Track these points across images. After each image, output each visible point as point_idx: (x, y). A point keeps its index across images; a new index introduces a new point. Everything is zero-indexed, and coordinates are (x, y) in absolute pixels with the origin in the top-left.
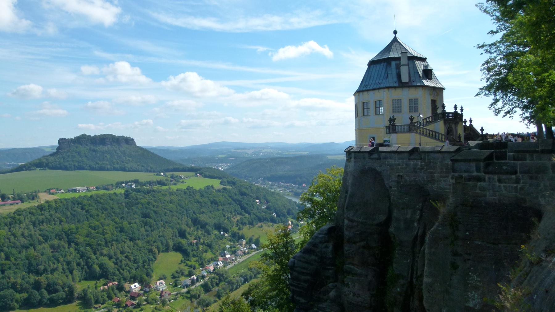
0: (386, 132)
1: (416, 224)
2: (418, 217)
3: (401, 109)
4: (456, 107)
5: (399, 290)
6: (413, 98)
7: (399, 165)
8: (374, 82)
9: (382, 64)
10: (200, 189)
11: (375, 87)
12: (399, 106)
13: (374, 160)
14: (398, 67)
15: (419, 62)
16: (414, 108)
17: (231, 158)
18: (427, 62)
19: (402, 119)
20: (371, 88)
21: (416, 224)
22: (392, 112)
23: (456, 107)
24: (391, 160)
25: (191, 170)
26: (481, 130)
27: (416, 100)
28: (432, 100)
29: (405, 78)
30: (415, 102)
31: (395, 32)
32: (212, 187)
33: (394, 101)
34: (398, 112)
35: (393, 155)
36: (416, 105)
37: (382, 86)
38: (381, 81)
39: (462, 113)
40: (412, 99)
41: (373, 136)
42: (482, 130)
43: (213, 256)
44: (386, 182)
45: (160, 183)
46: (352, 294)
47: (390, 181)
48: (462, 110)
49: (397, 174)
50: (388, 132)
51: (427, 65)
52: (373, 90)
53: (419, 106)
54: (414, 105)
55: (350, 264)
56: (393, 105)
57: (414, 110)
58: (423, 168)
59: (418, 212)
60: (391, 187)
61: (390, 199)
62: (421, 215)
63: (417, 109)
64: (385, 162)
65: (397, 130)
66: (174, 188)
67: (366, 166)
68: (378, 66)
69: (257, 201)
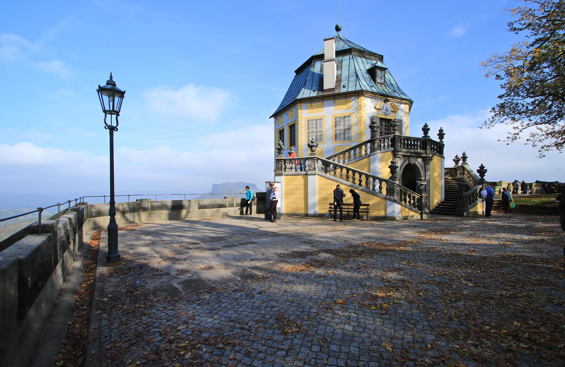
4: (426, 129)
12: (318, 129)
23: (426, 129)
26: (478, 171)
33: (310, 122)
39: (441, 141)
42: (482, 171)
48: (441, 135)
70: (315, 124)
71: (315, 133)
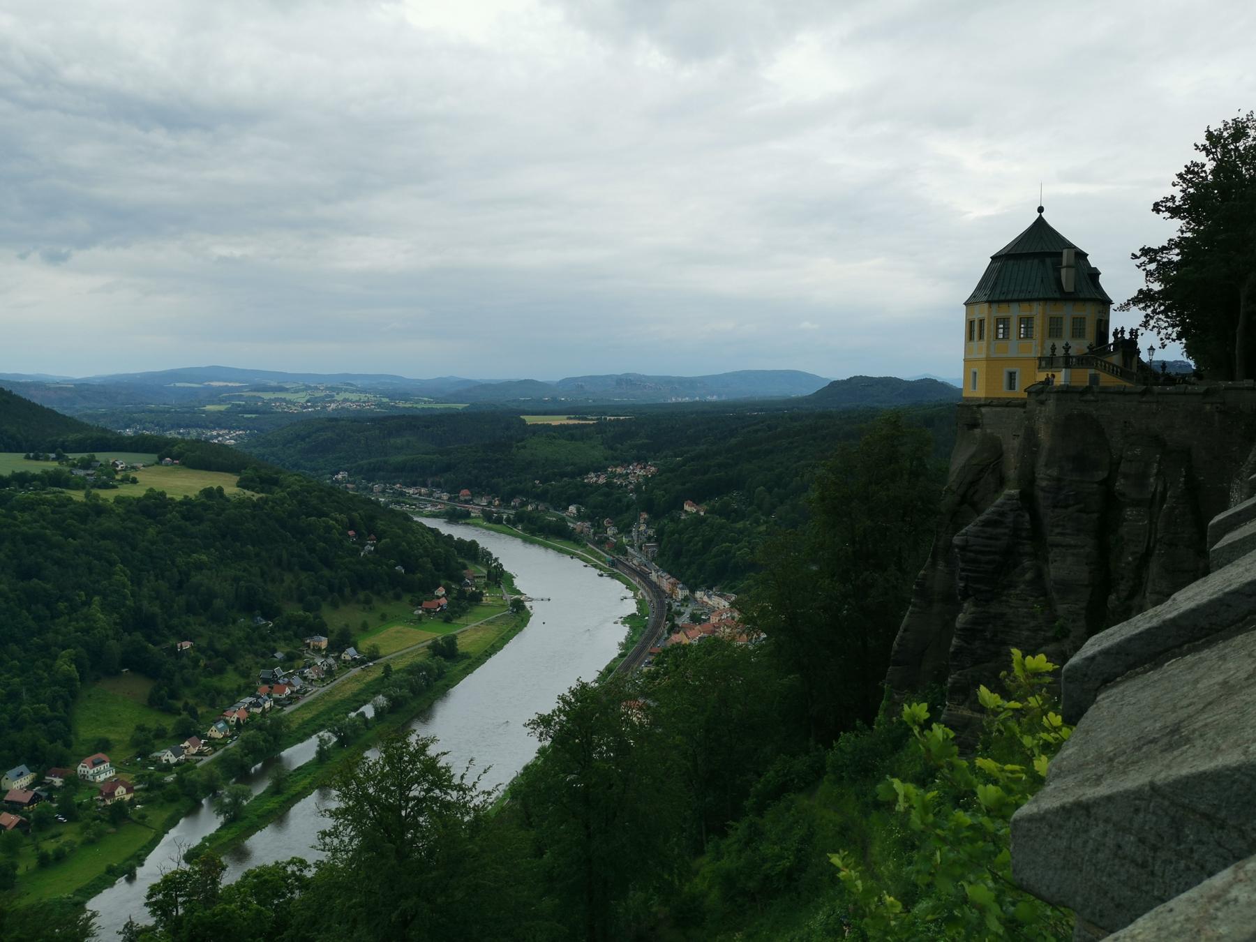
0: (1037, 366)
10: (186, 497)
11: (1022, 296)
14: (1057, 268)
17: (246, 416)
20: (1015, 297)
21: (1152, 480)
25: (139, 445)
29: (1068, 286)
31: (1041, 210)
32: (220, 490)
37: (1035, 295)
41: (1012, 369)
43: (242, 681)
45: (56, 480)
52: (1018, 301)
55: (1058, 534)
59: (1156, 465)
66: (108, 495)
69: (351, 533)
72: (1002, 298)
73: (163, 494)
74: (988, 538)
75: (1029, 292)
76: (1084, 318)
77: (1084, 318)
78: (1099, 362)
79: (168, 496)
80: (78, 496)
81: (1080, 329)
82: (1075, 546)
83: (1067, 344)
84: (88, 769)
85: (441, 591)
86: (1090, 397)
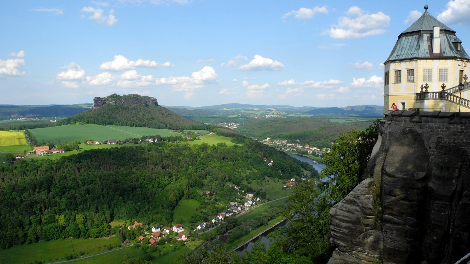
1: (454, 181)
2: (456, 175)
3: (431, 78)
5: (435, 238)
6: (443, 68)
7: (439, 128)
8: (406, 53)
9: (415, 36)
11: (407, 57)
12: (430, 75)
13: (415, 123)
15: (449, 35)
16: (443, 77)
17: (241, 119)
18: (455, 36)
19: (435, 87)
20: (403, 58)
21: (454, 181)
22: (423, 80)
24: (431, 124)
27: (446, 70)
28: (460, 70)
29: (436, 50)
30: (444, 72)
31: (426, 8)
33: (425, 70)
34: (428, 80)
35: (434, 119)
36: (445, 75)
38: (413, 52)
40: (442, 69)
41: (403, 101)
44: (426, 143)
46: (389, 240)
47: (430, 142)
49: (437, 136)
50: (419, 98)
51: (456, 38)
53: (448, 77)
54: (443, 75)
56: (424, 74)
57: (443, 79)
58: (463, 132)
60: (430, 148)
61: (429, 158)
62: (460, 174)
63: (447, 78)
64: (426, 124)
65: (429, 97)
67: (407, 128)
68: (410, 38)
70: (428, 72)
71: (428, 76)
72: (397, 58)
73: (207, 144)
74: (346, 211)
75: (411, 54)
76: (447, 69)
77: (447, 69)
78: (455, 98)
79: (208, 145)
80: (183, 143)
81: (429, 76)
82: (398, 224)
83: (443, 85)
84: (176, 228)
85: (293, 180)
86: (416, 119)
